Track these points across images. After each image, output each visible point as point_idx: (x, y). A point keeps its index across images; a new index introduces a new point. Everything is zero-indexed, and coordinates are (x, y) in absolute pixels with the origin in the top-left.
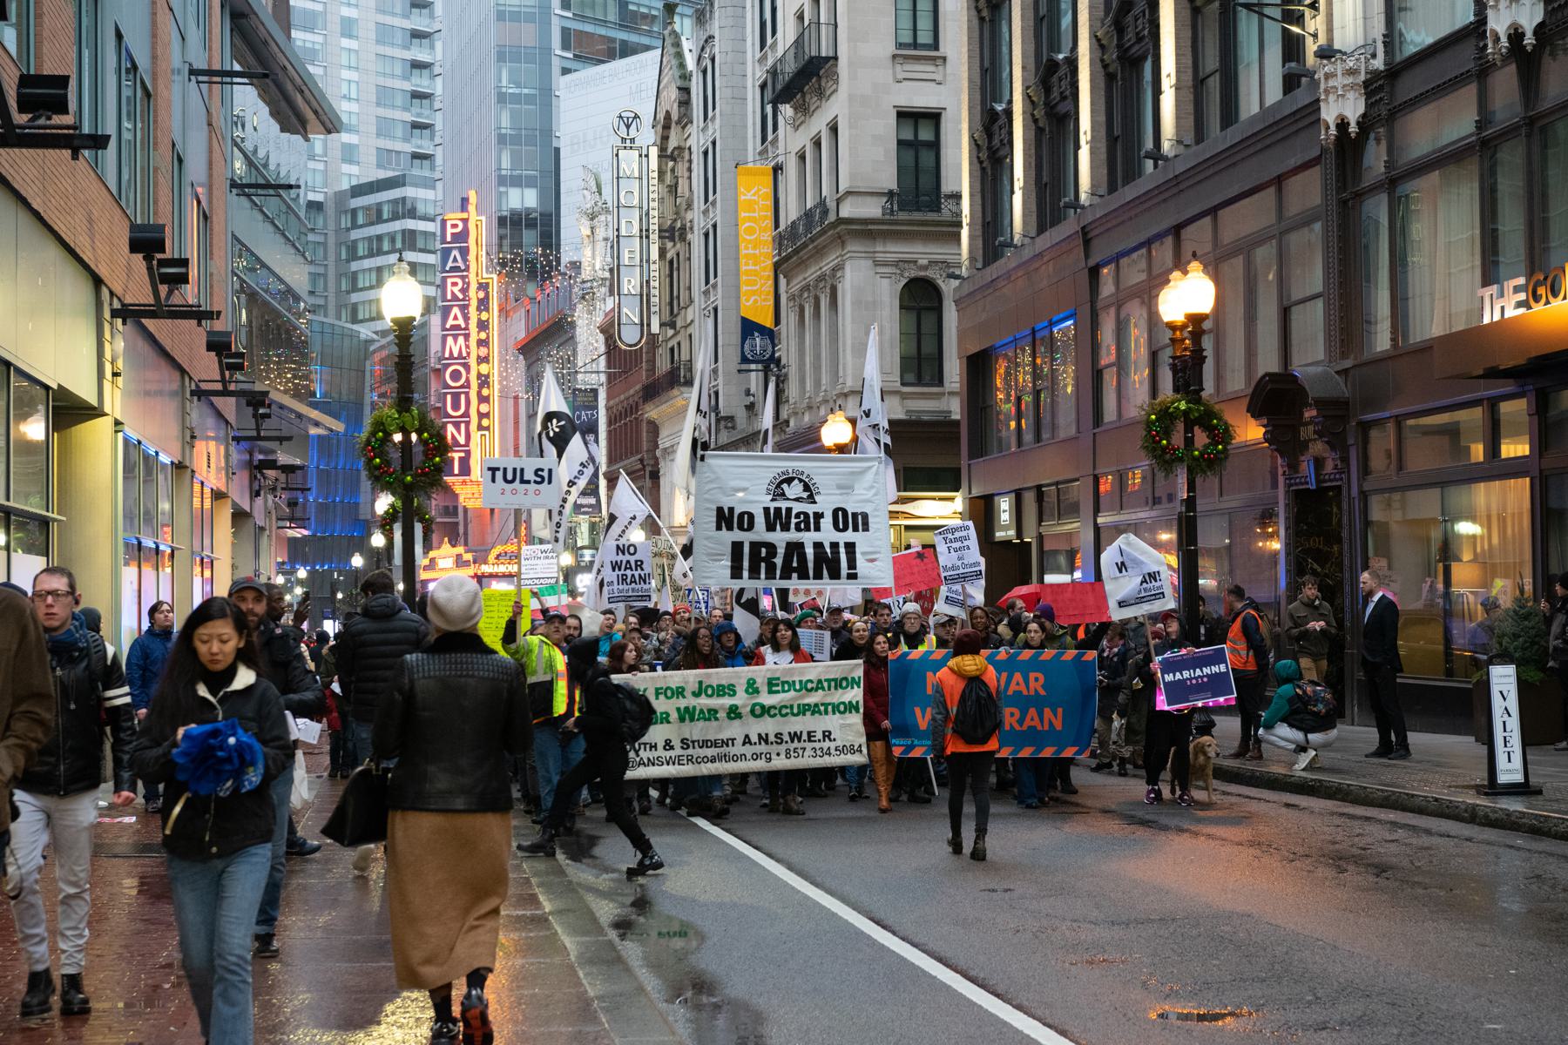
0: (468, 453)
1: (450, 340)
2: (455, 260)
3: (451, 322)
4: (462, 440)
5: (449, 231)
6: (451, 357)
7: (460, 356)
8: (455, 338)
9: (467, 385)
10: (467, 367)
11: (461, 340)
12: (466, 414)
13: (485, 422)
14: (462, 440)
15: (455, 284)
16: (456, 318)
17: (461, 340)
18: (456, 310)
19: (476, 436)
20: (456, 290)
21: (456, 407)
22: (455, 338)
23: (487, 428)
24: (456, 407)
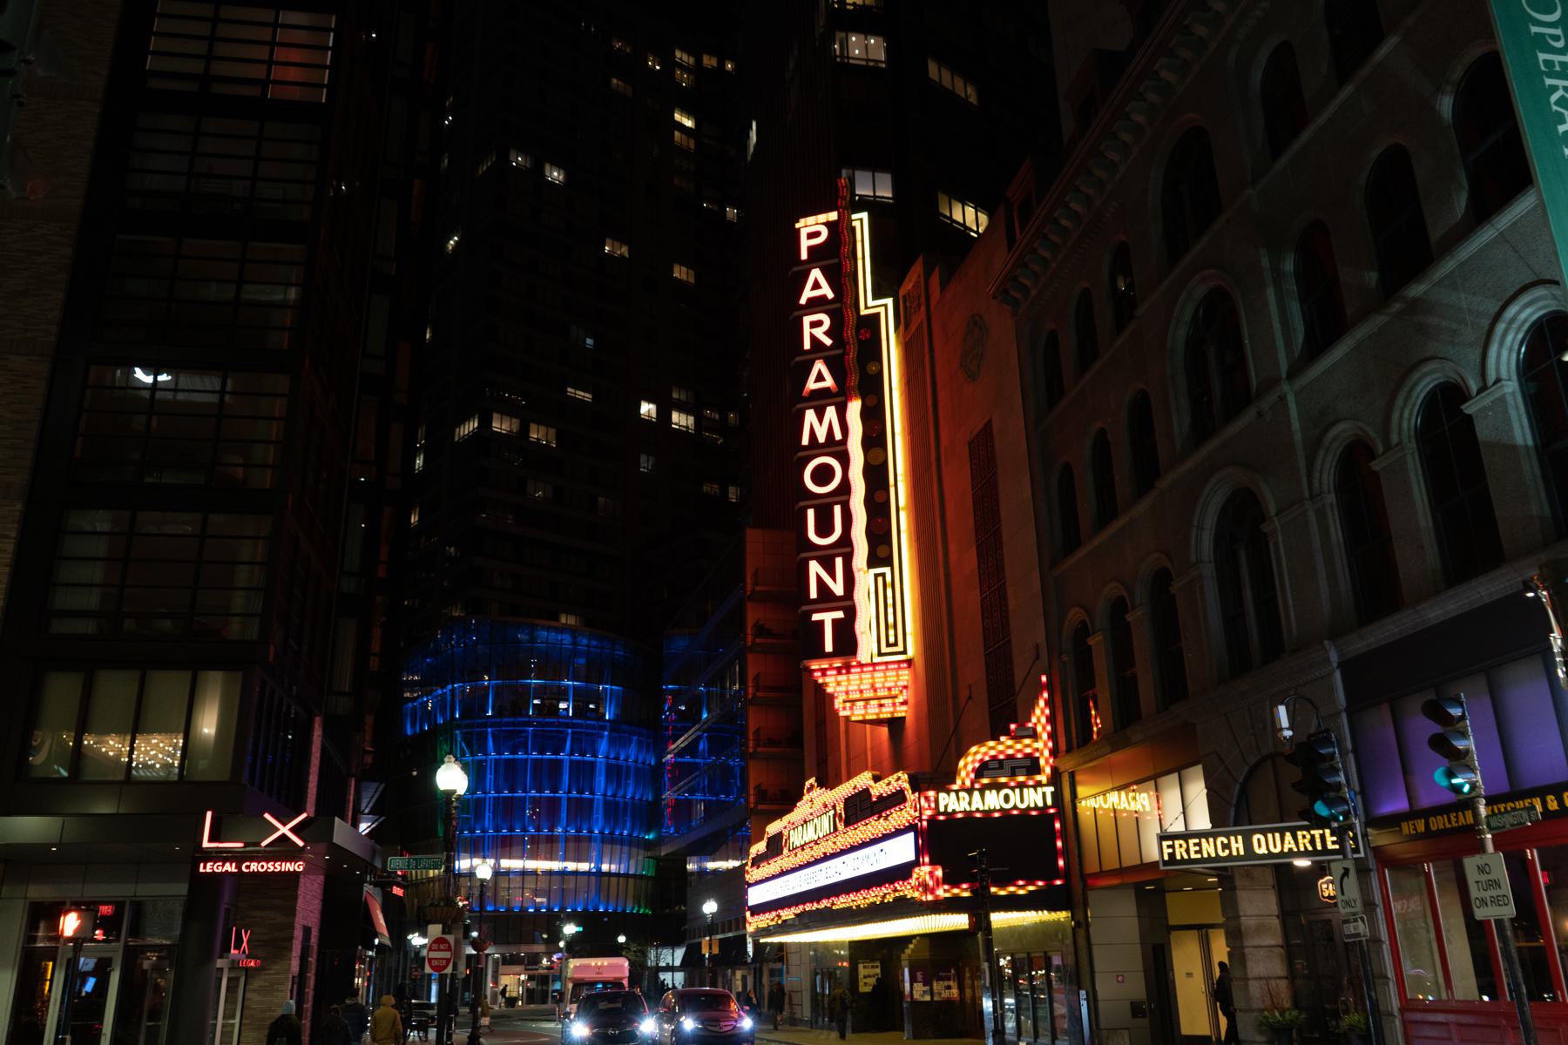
0: (851, 612)
2: (816, 286)
4: (838, 589)
5: (805, 243)
9: (845, 487)
10: (845, 461)
11: (831, 412)
12: (846, 541)
14: (838, 589)
15: (818, 324)
17: (831, 412)
18: (819, 366)
19: (865, 579)
20: (819, 333)
21: (824, 528)
23: (888, 562)
24: (824, 528)
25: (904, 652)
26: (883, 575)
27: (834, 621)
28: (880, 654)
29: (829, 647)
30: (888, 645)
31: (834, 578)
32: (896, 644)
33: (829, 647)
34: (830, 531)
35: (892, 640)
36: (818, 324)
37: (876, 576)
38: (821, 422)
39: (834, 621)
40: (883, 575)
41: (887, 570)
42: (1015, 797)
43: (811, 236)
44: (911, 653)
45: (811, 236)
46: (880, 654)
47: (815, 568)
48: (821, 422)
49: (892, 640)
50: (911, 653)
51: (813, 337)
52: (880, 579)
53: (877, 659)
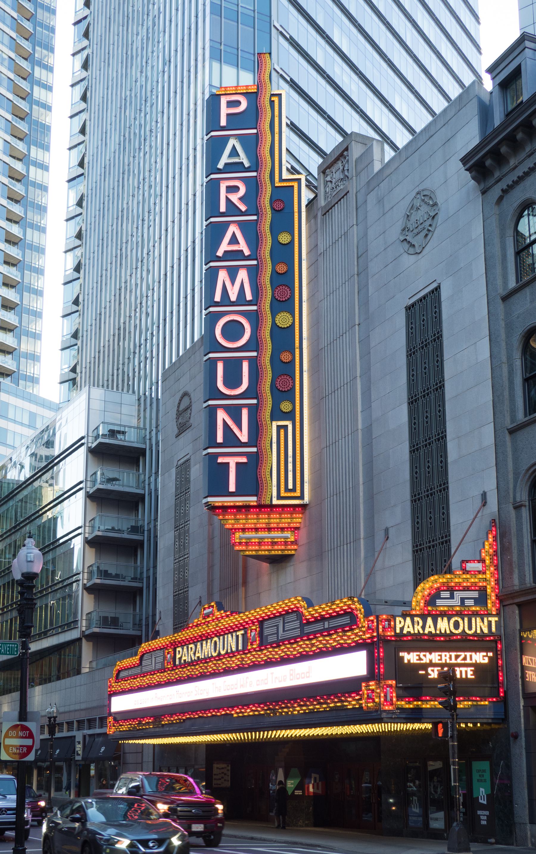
1: (223, 275)
2: (234, 153)
3: (224, 247)
5: (224, 111)
6: (226, 300)
7: (241, 300)
8: (233, 273)
11: (243, 275)
13: (286, 407)
15: (236, 189)
16: (234, 240)
20: (234, 198)
21: (233, 380)
22: (233, 273)
23: (290, 416)
24: (233, 380)
25: (302, 497)
26: (286, 427)
27: (238, 464)
28: (279, 497)
29: (232, 488)
30: (287, 490)
31: (240, 428)
32: (294, 490)
33: (232, 488)
34: (239, 383)
35: (290, 486)
36: (236, 189)
37: (279, 427)
38: (233, 282)
39: (238, 464)
40: (286, 427)
41: (289, 424)
42: (464, 625)
43: (231, 104)
44: (307, 499)
45: (231, 104)
46: (279, 497)
47: (221, 416)
48: (233, 282)
49: (290, 486)
50: (307, 499)
51: (228, 200)
52: (282, 432)
53: (275, 502)
